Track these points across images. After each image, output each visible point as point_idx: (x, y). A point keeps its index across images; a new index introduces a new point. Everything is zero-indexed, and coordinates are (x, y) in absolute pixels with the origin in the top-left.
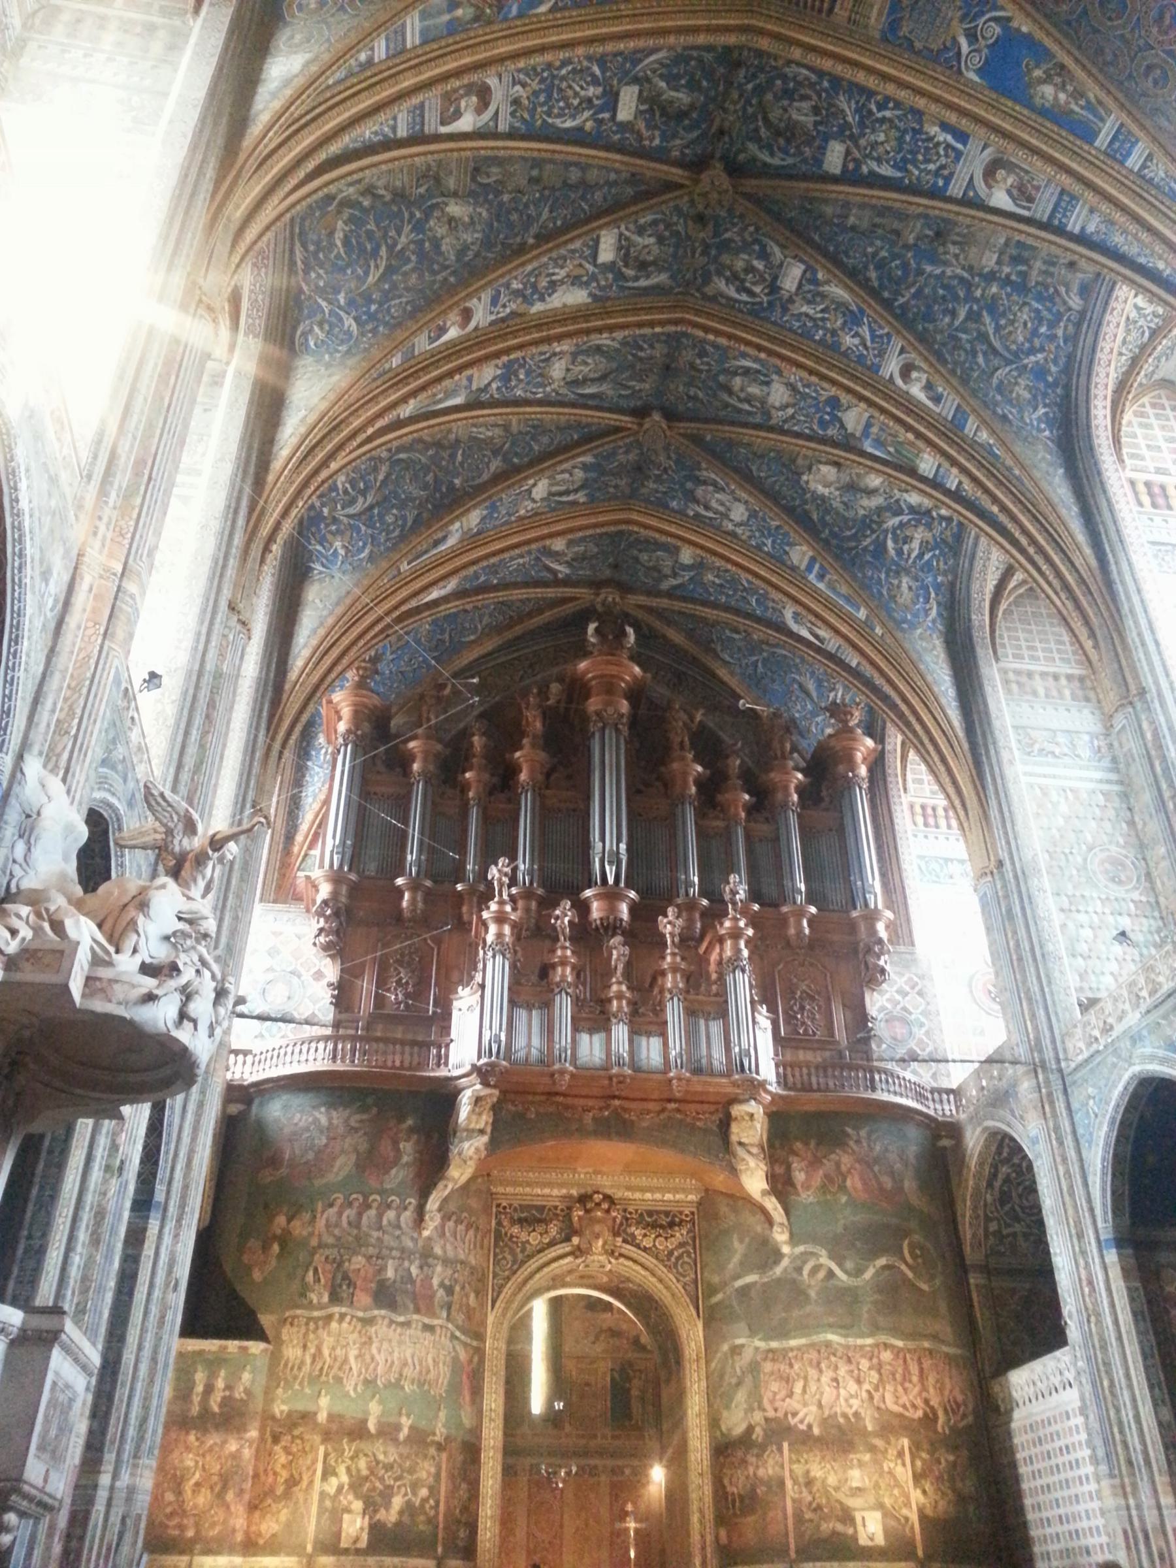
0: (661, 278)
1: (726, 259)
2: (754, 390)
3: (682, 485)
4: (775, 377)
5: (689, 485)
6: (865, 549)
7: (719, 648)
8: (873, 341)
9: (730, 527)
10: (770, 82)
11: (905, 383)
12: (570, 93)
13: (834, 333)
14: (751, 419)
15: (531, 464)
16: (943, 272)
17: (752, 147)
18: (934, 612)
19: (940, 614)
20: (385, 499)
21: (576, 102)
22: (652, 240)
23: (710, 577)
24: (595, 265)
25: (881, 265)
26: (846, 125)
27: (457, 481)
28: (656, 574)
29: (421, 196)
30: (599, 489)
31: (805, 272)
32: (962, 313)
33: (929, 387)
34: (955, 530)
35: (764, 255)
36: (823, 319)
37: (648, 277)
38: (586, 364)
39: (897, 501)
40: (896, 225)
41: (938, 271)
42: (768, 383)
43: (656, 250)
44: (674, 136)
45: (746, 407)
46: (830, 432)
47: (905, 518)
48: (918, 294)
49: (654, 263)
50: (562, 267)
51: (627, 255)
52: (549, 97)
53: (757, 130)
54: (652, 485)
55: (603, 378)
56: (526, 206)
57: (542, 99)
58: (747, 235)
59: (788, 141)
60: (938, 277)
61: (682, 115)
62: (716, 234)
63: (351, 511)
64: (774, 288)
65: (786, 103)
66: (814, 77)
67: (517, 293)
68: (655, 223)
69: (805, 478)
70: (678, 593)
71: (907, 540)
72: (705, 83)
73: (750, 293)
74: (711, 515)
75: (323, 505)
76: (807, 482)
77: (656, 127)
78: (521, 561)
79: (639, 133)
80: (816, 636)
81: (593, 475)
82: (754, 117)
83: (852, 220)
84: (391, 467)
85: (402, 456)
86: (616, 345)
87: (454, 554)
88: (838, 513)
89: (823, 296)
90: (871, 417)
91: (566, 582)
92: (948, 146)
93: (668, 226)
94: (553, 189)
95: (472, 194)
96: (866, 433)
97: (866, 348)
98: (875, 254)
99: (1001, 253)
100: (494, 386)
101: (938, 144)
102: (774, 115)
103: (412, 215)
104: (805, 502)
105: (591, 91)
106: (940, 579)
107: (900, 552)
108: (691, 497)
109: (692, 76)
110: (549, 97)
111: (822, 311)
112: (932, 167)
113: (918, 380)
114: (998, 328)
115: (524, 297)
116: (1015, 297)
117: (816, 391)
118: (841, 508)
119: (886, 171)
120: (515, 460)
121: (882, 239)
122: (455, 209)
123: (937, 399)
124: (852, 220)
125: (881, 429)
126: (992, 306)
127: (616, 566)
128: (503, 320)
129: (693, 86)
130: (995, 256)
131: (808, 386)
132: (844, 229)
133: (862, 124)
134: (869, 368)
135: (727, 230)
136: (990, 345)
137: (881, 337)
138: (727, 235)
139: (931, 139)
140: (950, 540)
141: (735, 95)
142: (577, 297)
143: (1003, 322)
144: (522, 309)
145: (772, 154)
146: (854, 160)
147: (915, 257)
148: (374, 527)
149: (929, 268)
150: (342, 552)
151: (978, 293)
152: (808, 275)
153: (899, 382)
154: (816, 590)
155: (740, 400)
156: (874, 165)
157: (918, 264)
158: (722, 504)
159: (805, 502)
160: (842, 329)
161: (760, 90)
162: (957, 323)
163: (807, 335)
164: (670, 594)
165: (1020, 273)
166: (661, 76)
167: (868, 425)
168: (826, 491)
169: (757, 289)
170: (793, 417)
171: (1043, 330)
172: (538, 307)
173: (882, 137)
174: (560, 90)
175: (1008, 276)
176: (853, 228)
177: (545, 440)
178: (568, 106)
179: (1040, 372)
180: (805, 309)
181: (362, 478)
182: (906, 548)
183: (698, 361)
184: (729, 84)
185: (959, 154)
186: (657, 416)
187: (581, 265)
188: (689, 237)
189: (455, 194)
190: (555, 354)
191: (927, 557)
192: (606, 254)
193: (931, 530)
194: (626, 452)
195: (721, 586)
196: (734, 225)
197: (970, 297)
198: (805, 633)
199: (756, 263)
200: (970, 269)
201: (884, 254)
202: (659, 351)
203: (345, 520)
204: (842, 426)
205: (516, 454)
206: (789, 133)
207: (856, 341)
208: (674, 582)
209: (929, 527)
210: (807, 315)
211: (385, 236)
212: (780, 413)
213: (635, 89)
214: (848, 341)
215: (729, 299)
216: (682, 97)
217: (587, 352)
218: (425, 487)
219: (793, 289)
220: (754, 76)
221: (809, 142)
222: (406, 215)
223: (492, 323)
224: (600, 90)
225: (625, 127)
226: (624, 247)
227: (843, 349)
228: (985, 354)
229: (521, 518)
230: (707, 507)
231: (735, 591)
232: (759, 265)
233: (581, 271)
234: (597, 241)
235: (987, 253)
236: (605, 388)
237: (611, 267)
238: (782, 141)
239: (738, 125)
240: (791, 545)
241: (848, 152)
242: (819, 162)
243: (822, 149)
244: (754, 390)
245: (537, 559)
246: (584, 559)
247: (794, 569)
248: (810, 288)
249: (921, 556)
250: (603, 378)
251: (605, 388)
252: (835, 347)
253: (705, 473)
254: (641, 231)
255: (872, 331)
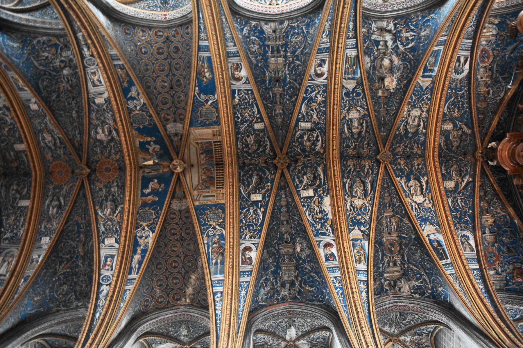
0: (320, 169)
1: (308, 149)
2: (356, 124)
3: (411, 138)
4: (347, 118)
5: (410, 135)
6: (413, 56)
7: (499, 98)
8: (315, 90)
9: (424, 114)
10: (246, 152)
11: (324, 74)
12: (251, 218)
13: (319, 104)
14: (369, 121)
15: (404, 206)
16: (289, 74)
17: (267, 151)
18: (433, 15)
19: (433, 13)
20: (422, 267)
21: (254, 216)
22: (305, 177)
23: (456, 114)
24: (314, 196)
25: (291, 97)
26: (248, 125)
27: (413, 237)
28: (464, 137)
29: (296, 260)
30: (420, 173)
31: (302, 122)
32: (298, 62)
33: (320, 65)
34: (399, 20)
35: (302, 137)
36: (316, 110)
37: (320, 175)
38: (356, 192)
39: (392, 49)
40: (278, 96)
41: (288, 76)
42: (351, 120)
43: (308, 175)
44: (267, 178)
45: (364, 124)
46: (360, 91)
47: (399, 43)
48: (295, 80)
49: (314, 174)
50: (314, 209)
51: (311, 185)
52: (252, 225)
53: (261, 152)
54: (416, 150)
55: (364, 183)
56: (295, 224)
57: (251, 228)
58: (297, 145)
59: (261, 141)
60: (290, 76)
61: (261, 178)
62: (300, 154)
63: (428, 281)
64: (312, 130)
65: (250, 146)
66: (239, 140)
67: (323, 225)
68: (298, 178)
69: (392, 91)
70: (470, 126)
71: (407, 39)
72: (250, 172)
73: (317, 136)
74: (422, 123)
75: (427, 292)
76: (393, 89)
77: (264, 186)
78: (459, 201)
79: (266, 192)
80: (465, 61)
81: (412, 176)
82: (258, 154)
83: (281, 112)
84: (411, 263)
85: (406, 259)
86: (348, 181)
87: (446, 237)
88: (403, 72)
89: (307, 113)
90: (345, 79)
91: (474, 177)
92: (238, 94)
93: (299, 172)
94: (289, 215)
95: (294, 243)
96: (353, 79)
97: (319, 92)
98: (289, 100)
99: (278, 57)
100: (362, 228)
101: (239, 97)
102: (256, 148)
103: (301, 264)
104: (401, 87)
105: (251, 211)
106: (420, 18)
107: (412, 40)
108: (416, 133)
109: (248, 177)
110: (252, 225)
111: (313, 111)
112: (247, 97)
113: (320, 70)
114: (299, 48)
115: (324, 222)
116: (289, 46)
117: (346, 102)
118: (400, 71)
119: (255, 109)
120: (403, 212)
121: (283, 99)
122: (298, 249)
123: (324, 61)
124: (281, 112)
125: (348, 74)
126: (293, 52)
127: (465, 154)
128: (333, 230)
129: (251, 176)
130: (279, 58)
131: (345, 105)
132: (284, 113)
133: (246, 121)
134: (326, 87)
135: (297, 151)
136: (303, 48)
137: (312, 89)
138: (299, 151)
139: (239, 100)
140: (404, 20)
141: (253, 161)
142: (327, 201)
143: (297, 47)
144: (329, 222)
145: (267, 145)
146: (257, 119)
147: (286, 86)
148: (432, 273)
149: (288, 80)
150: (442, 288)
151: (291, 59)
152: (302, 120)
153: (325, 76)
154: (439, 70)
155: (363, 127)
156: (256, 113)
157: (287, 84)
158: (414, 120)
159: (401, 87)
160: (317, 102)
161: (250, 155)
162: (300, 63)
163: (325, 113)
164: (472, 128)
165: (282, 48)
166: (248, 187)
167: (349, 79)
168: (395, 80)
169: (315, 135)
170: (361, 106)
171: (296, 31)
172: (330, 216)
173: (246, 114)
174: (250, 222)
175: (284, 51)
176: (283, 110)
177: (395, 200)
178: (255, 218)
179: (308, 25)
180: (315, 117)
181: (416, 275)
182: (410, 38)
183: (352, 147)
184: (250, 164)
185: (239, 90)
186: (378, 157)
187: (314, 202)
188: (304, 163)
189: (294, 249)
190: (351, 205)
191: (412, 27)
192: (310, 193)
193: (401, 30)
194: (400, 164)
195: (458, 108)
196: (295, 150)
197: (293, 62)
198: (467, 66)
199: (305, 139)
200: (285, 65)
201: (288, 97)
202: (351, 163)
203: (432, 284)
204: (355, 87)
205: (401, 212)
206: (258, 142)
207: (318, 96)
208: (465, 129)
209: (400, 32)
210: (317, 116)
211: (308, 273)
212: (361, 111)
213: (252, 195)
214: (320, 98)
215: (322, 143)
216: (255, 179)
217: (351, 192)
218: (416, 250)
219: (310, 123)
220: (246, 157)
221: (259, 135)
222: (302, 266)
223: (333, 234)
224: (251, 208)
225: (264, 197)
226: (307, 187)
227: (324, 99)
228: (306, 50)
229: (434, 205)
230: (419, 125)
231: (459, 102)
232: (306, 137)
233: (317, 201)
234: (305, 198)
235: (279, 62)
236: (368, 181)
237: (315, 191)
238: (262, 143)
239: (261, 158)
240: (421, 88)
241: (256, 122)
242: (263, 130)
243: (259, 130)
244: (356, 124)
245: (459, 193)
246: (460, 170)
247: (433, 82)
248: (307, 118)
249: (412, 30)
250: (364, 183)
251: (368, 181)
252: (324, 102)
253: (402, 131)
254: (301, 182)
255: (311, 92)
